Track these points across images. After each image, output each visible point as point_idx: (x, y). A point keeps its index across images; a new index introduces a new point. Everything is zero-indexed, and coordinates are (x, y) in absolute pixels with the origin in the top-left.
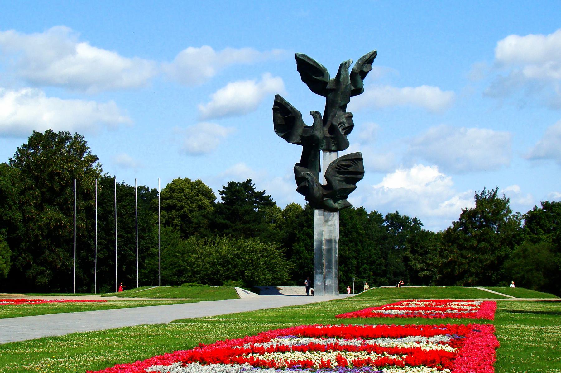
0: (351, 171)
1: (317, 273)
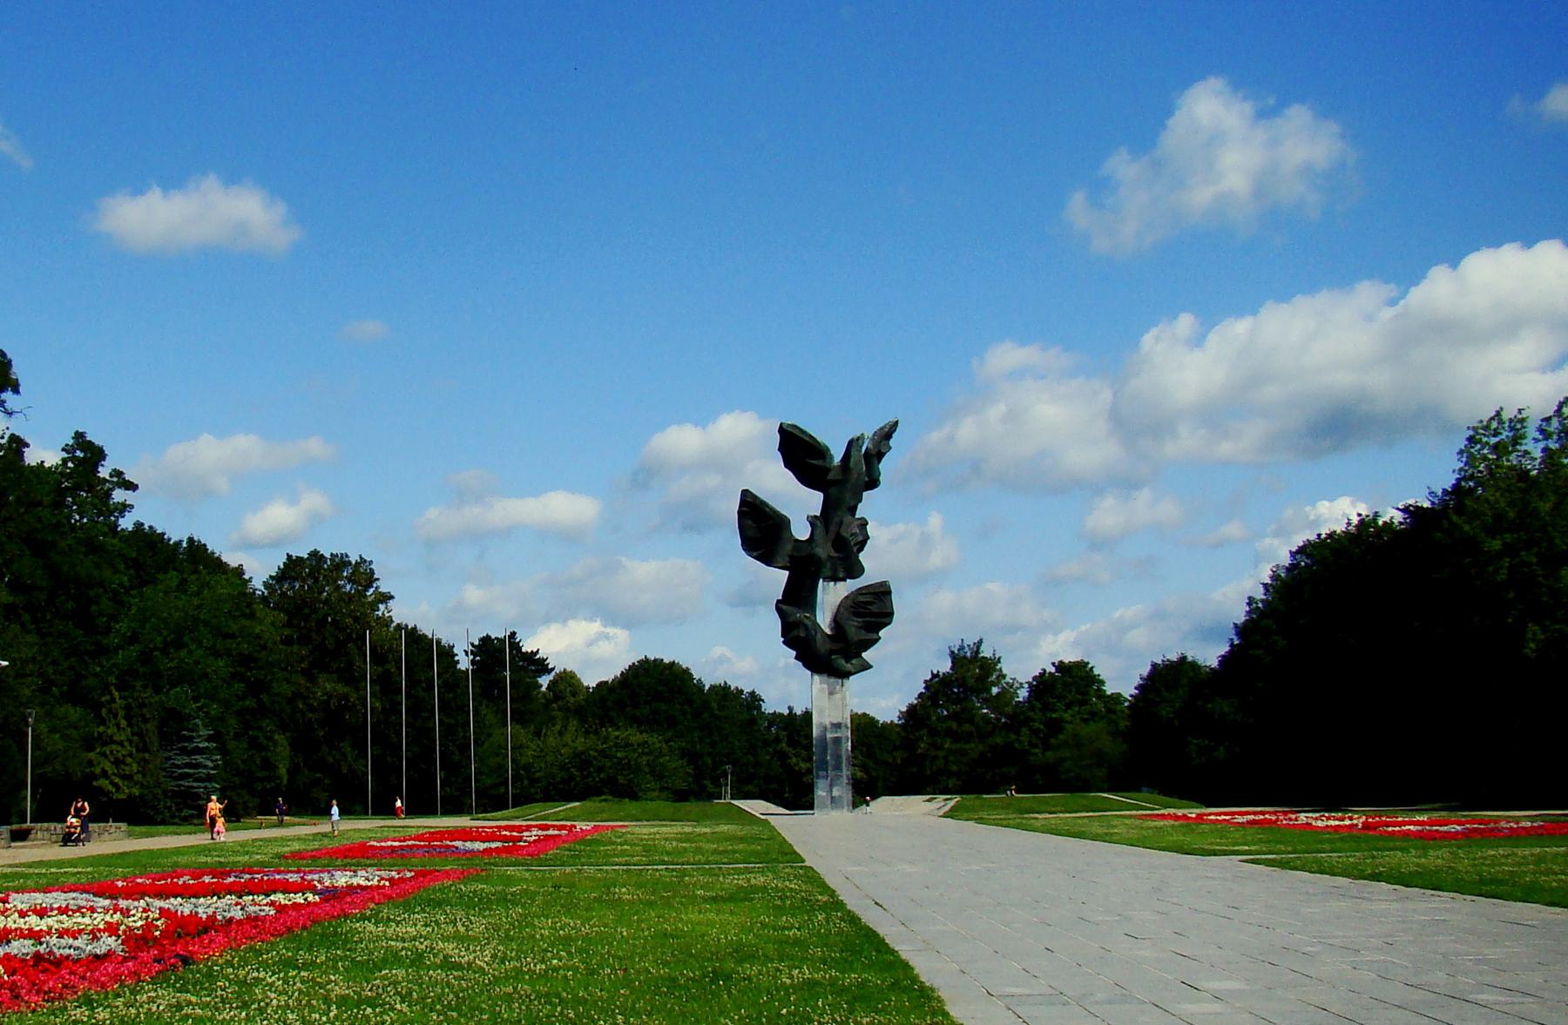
0: (873, 610)
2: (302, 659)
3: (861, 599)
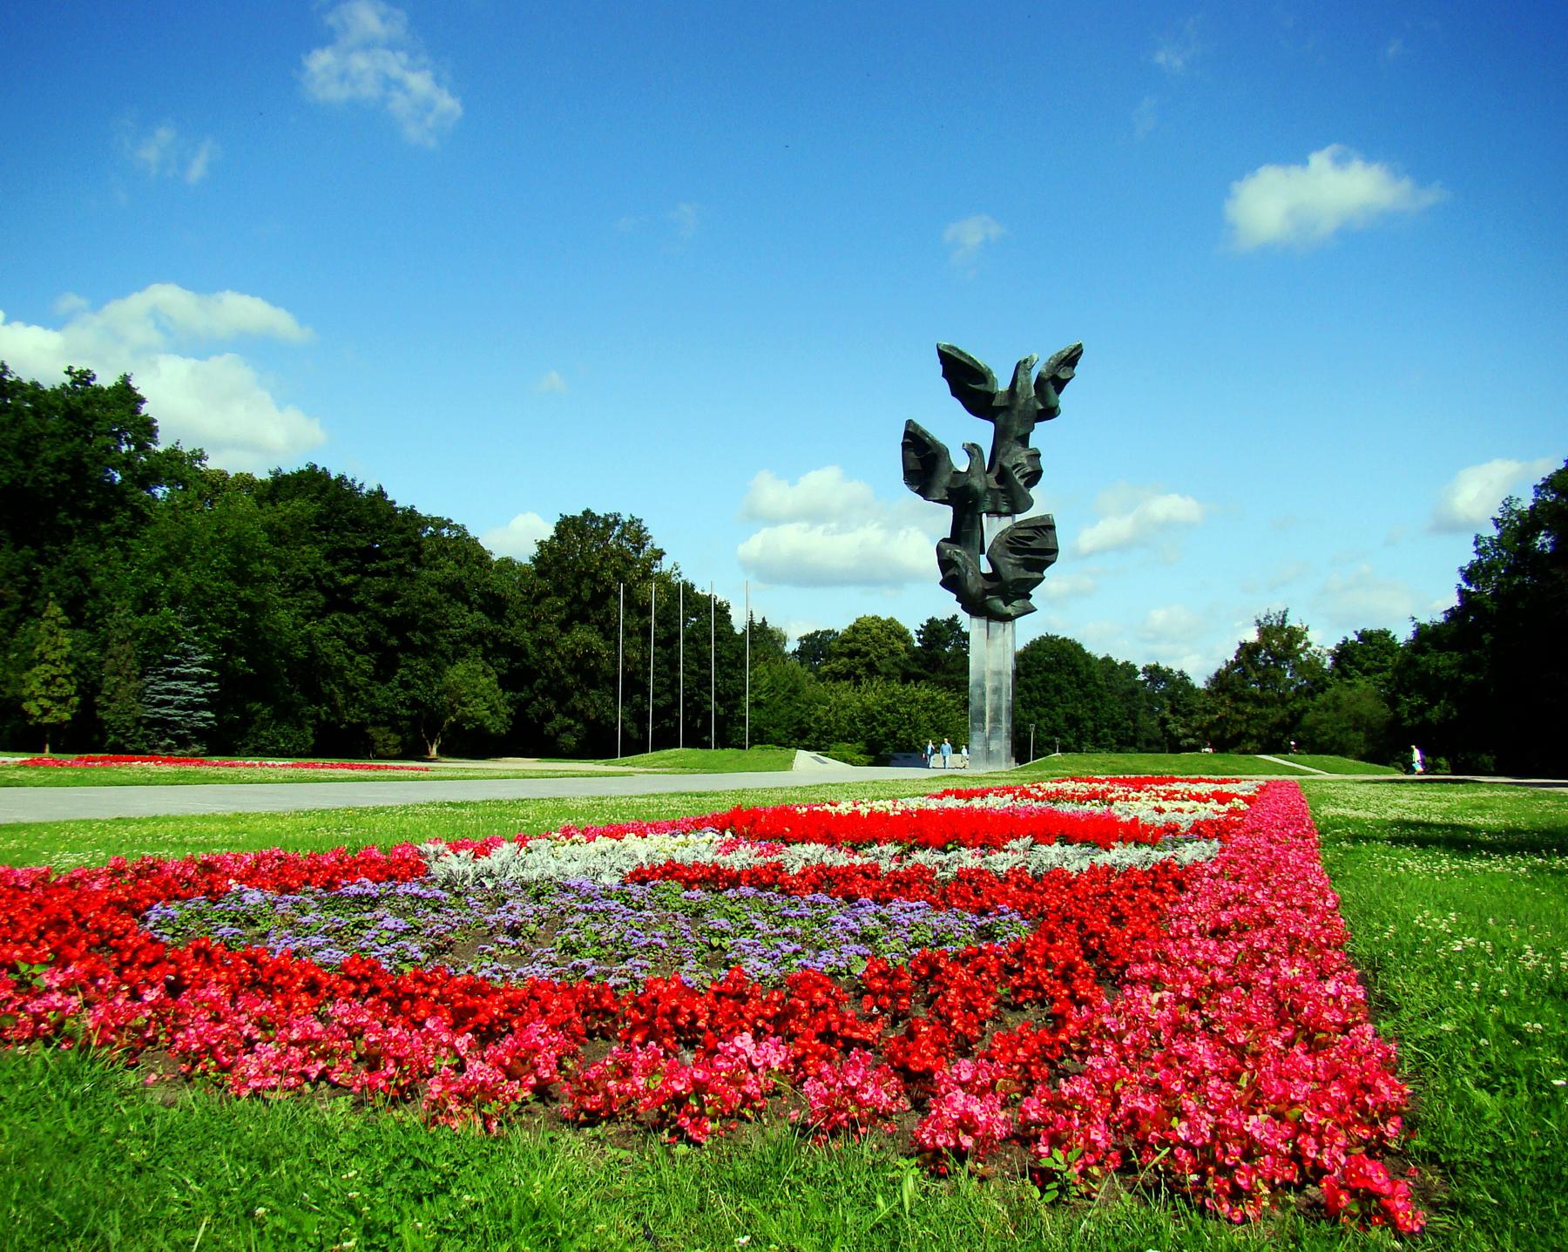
0: (1035, 549)
1: (974, 729)
2: (559, 610)
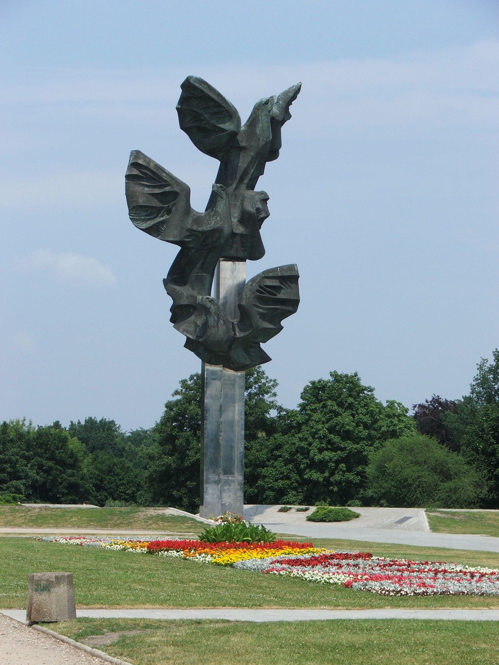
3: (269, 283)
